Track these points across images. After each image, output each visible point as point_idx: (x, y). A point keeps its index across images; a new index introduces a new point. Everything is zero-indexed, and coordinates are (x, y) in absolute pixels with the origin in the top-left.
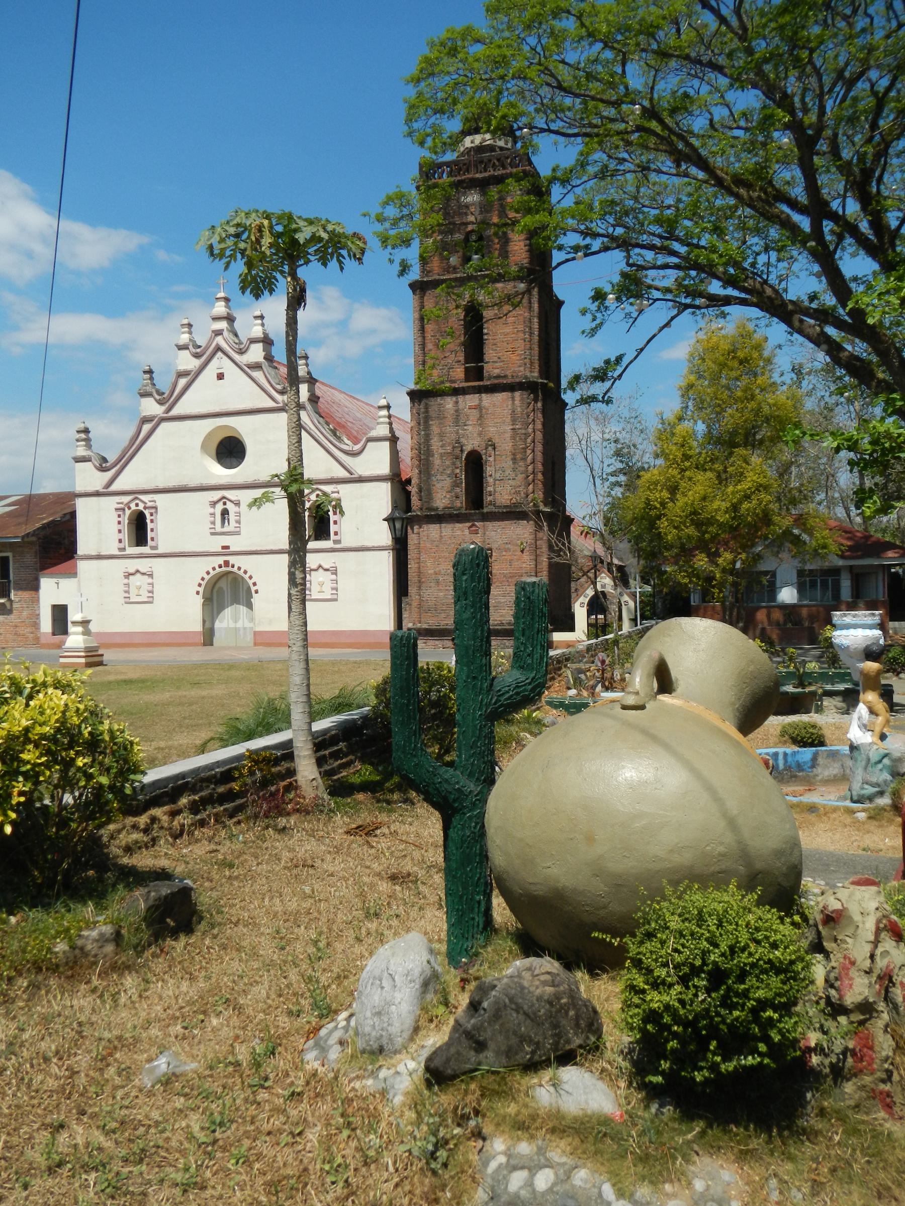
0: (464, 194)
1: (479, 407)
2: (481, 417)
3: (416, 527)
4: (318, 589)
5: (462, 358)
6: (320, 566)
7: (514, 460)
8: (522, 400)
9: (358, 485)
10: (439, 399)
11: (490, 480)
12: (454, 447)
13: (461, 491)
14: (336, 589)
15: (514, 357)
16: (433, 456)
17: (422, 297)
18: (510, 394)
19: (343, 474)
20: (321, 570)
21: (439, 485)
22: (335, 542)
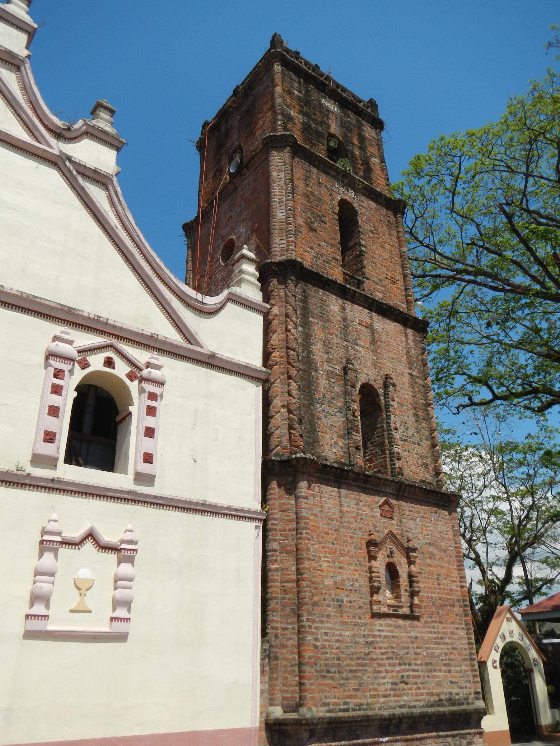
0: (325, 98)
1: (369, 326)
2: (373, 342)
3: (303, 484)
4: (74, 600)
5: (339, 258)
6: (91, 535)
7: (416, 415)
8: (415, 341)
9: (202, 371)
10: (321, 292)
11: (397, 436)
12: (345, 370)
13: (358, 437)
14: (127, 604)
15: (395, 289)
16: (316, 370)
17: (293, 158)
18: (402, 328)
19: (173, 336)
20: (89, 546)
21: (324, 420)
22: (140, 478)
